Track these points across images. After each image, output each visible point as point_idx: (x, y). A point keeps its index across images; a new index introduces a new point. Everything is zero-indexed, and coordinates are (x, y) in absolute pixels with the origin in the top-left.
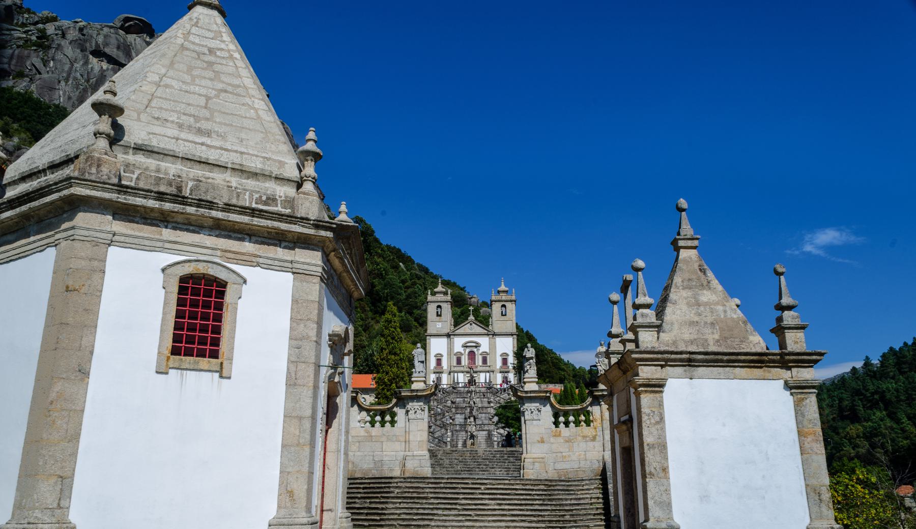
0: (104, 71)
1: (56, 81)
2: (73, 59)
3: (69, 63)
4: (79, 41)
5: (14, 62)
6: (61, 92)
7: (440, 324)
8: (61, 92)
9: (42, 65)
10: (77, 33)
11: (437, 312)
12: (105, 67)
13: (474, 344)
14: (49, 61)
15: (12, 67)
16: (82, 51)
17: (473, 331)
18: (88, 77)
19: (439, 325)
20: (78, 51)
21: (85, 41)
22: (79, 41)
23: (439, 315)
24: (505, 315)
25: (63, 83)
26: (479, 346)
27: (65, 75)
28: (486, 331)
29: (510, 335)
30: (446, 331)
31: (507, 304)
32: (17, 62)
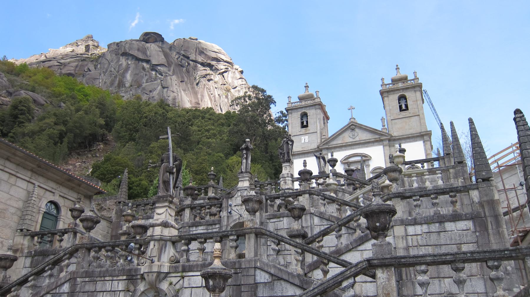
0: (129, 64)
1: (99, 74)
2: (111, 61)
3: (108, 63)
4: (116, 50)
5: (78, 69)
6: (101, 80)
7: (307, 137)
8: (101, 80)
9: (93, 68)
10: (115, 46)
11: (302, 123)
12: (129, 63)
13: (359, 158)
14: (98, 65)
15: (76, 72)
16: (116, 55)
17: (357, 139)
18: (118, 69)
19: (305, 139)
20: (114, 55)
21: (119, 49)
22: (116, 50)
23: (304, 126)
24: (407, 108)
25: (103, 75)
26: (368, 160)
27: (105, 70)
28: (377, 137)
29: (417, 136)
30: (314, 146)
31: (408, 94)
32: (80, 69)
